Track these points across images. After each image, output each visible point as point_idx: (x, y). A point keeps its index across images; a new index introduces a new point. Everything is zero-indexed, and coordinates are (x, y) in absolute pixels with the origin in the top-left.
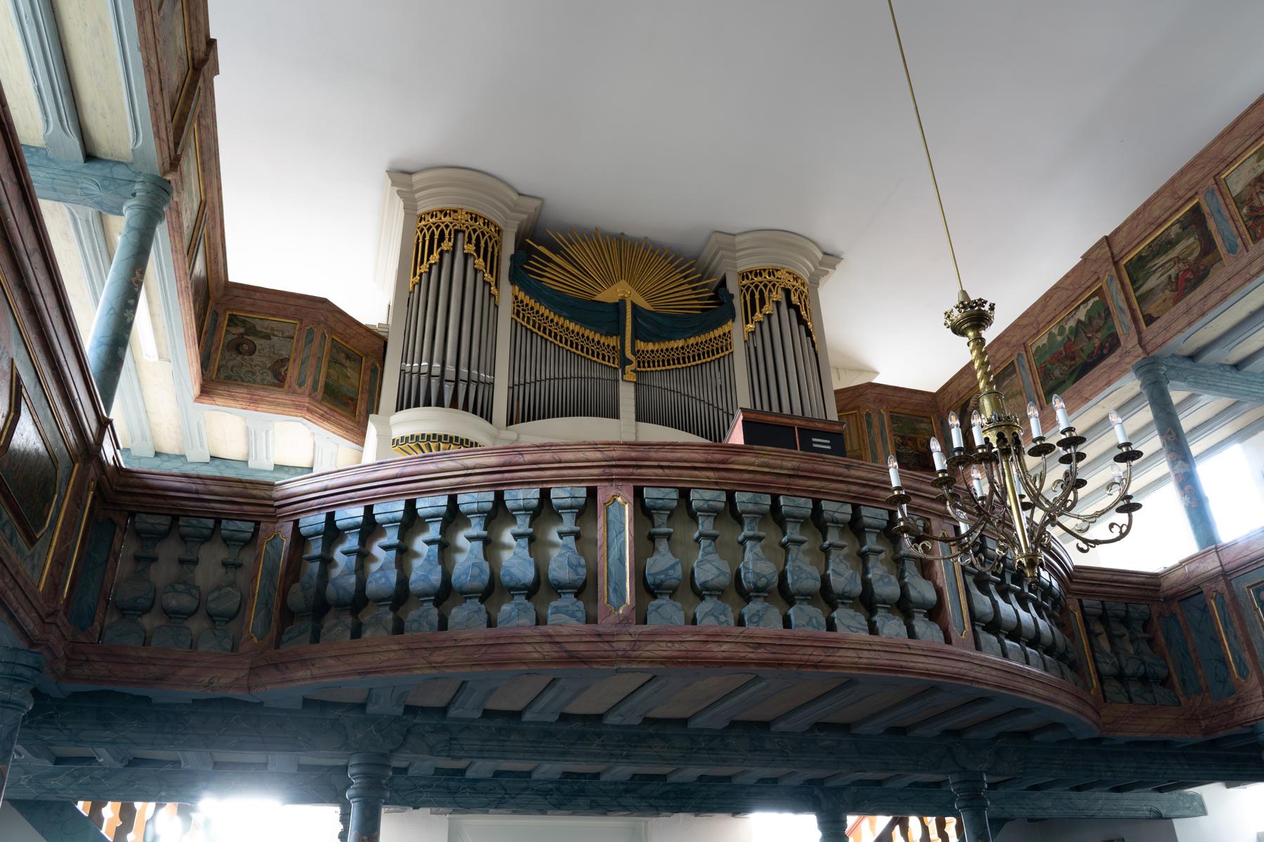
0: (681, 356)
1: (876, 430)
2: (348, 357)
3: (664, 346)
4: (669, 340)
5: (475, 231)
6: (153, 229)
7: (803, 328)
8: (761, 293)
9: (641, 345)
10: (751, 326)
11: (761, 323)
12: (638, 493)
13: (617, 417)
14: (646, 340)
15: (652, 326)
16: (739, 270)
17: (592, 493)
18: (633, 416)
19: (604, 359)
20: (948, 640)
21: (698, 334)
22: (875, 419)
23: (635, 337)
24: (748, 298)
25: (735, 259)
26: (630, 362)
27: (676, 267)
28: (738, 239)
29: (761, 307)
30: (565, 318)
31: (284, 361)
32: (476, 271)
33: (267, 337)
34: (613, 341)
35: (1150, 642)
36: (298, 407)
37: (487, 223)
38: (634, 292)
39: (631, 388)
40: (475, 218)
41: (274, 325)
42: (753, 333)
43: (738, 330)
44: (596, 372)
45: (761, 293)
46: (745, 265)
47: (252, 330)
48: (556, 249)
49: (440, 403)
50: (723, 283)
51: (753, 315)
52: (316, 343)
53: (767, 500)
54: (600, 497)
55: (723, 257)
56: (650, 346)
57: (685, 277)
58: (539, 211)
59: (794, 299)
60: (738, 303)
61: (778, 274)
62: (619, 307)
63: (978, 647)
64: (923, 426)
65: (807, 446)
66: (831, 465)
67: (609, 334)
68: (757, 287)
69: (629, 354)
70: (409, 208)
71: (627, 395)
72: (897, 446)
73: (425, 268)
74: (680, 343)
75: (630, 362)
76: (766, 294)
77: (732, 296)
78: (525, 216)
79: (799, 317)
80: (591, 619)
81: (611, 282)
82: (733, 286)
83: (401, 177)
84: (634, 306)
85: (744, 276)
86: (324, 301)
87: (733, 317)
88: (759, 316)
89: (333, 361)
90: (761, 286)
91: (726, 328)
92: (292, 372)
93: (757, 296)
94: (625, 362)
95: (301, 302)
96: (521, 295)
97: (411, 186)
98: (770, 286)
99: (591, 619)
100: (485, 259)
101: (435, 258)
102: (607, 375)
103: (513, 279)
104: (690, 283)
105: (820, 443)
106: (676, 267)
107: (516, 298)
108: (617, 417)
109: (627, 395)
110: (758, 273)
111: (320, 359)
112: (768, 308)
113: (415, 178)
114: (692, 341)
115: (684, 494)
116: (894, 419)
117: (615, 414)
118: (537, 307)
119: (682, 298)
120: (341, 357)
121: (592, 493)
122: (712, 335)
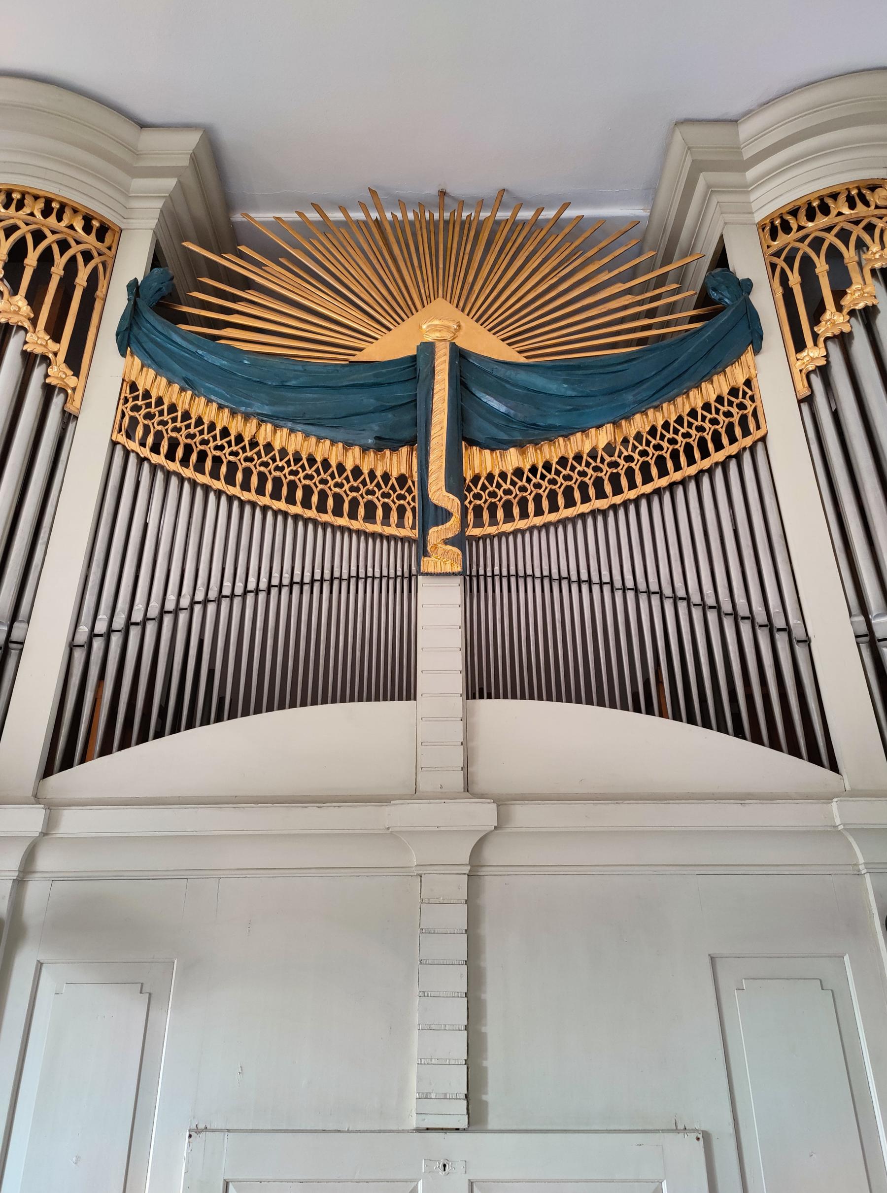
0: (606, 473)
3: (551, 452)
4: (567, 432)
5: (39, 236)
8: (834, 256)
9: (480, 461)
10: (813, 355)
11: (844, 340)
13: (409, 693)
14: (496, 445)
16: (759, 217)
18: (457, 683)
19: (370, 516)
23: (463, 434)
24: (794, 279)
25: (744, 189)
26: (443, 516)
28: (746, 130)
29: (839, 295)
30: (263, 419)
34: (397, 463)
38: (468, 323)
39: (454, 591)
42: (824, 371)
43: (773, 374)
44: (347, 556)
45: (834, 256)
48: (275, 254)
50: (721, 259)
51: (815, 320)
55: (711, 190)
56: (512, 459)
57: (651, 313)
60: (766, 302)
62: (414, 369)
67: (385, 443)
68: (817, 243)
69: (439, 493)
74: (602, 437)
75: (443, 516)
76: (849, 255)
77: (747, 286)
78: (170, 183)
81: (402, 309)
82: (748, 261)
84: (459, 356)
85: (775, 227)
87: (755, 338)
88: (834, 321)
90: (831, 238)
91: (737, 375)
93: (822, 267)
96: (147, 379)
98: (857, 231)
100: (34, 298)
102: (383, 560)
107: (133, 387)
108: (409, 693)
109: (440, 614)
110: (817, 207)
114: (639, 424)
117: (400, 684)
118: (183, 401)
119: (605, 319)
122: (696, 399)
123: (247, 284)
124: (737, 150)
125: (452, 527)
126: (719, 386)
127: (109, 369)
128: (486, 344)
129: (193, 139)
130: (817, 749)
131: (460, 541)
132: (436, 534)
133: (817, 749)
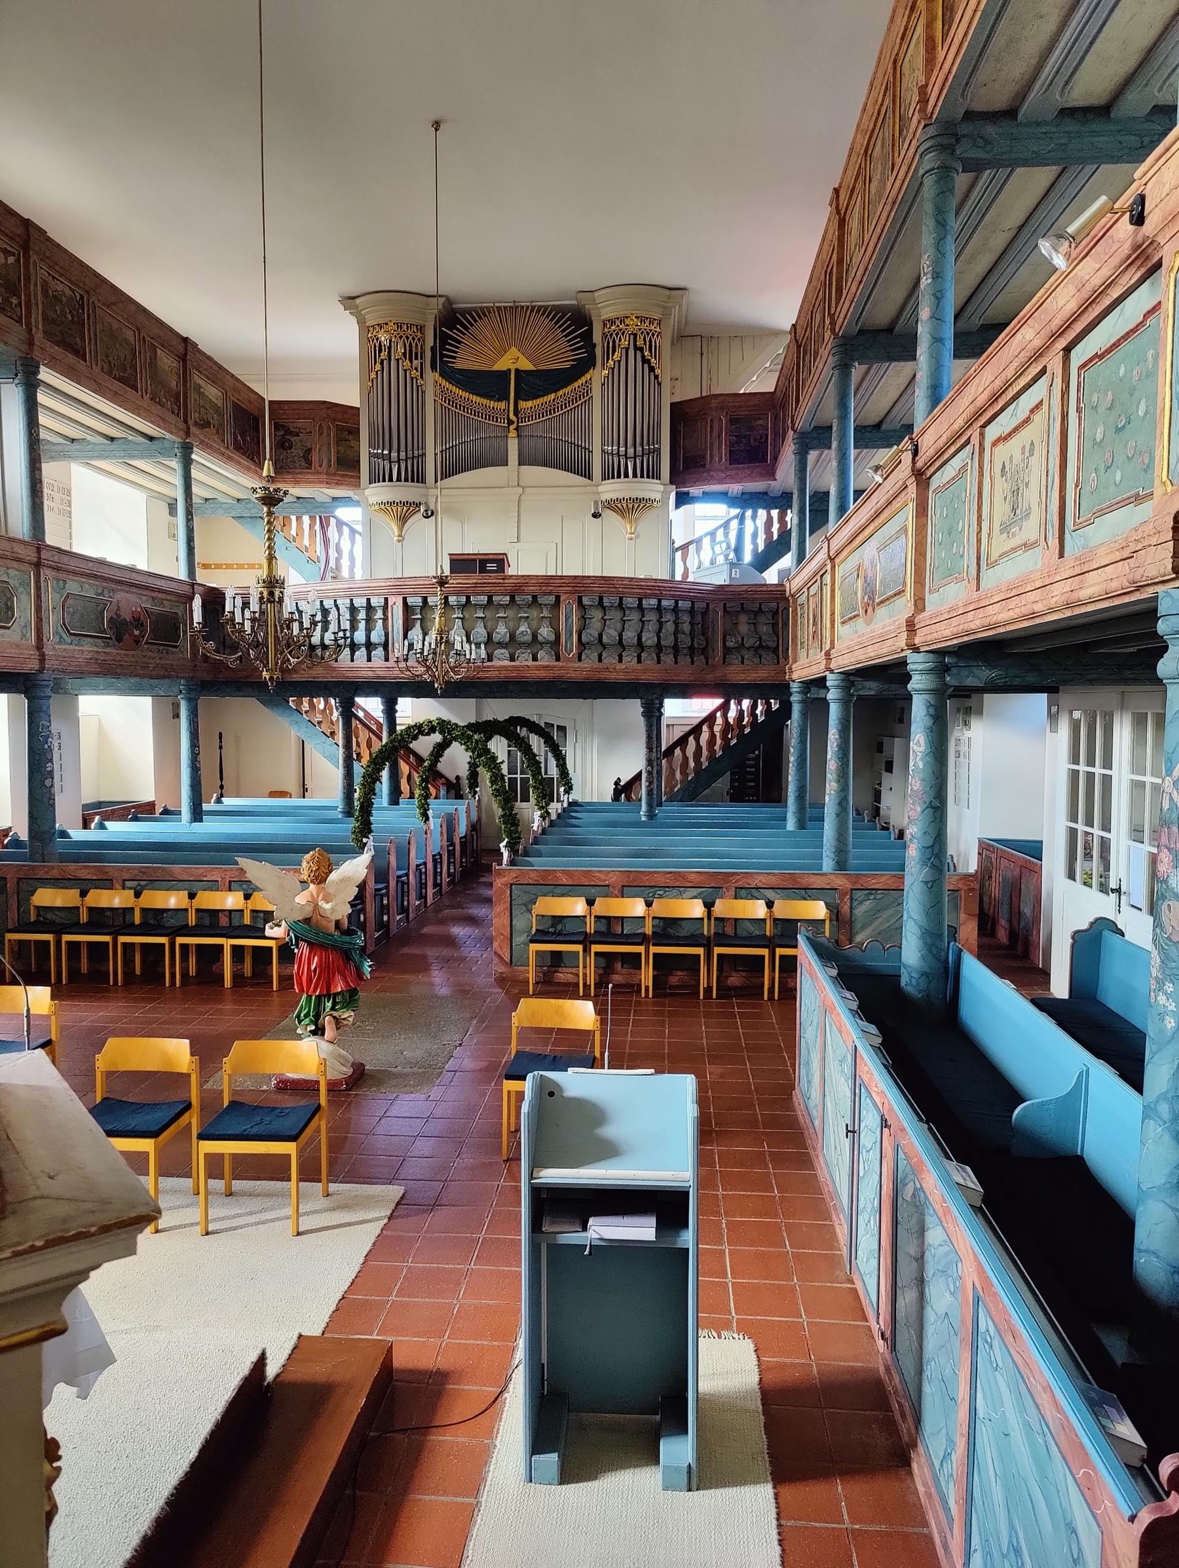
1: (715, 434)
2: (350, 433)
3: (539, 401)
6: (190, 471)
7: (646, 366)
9: (523, 405)
12: (405, 599)
15: (535, 384)
17: (386, 599)
18: (517, 463)
20: (558, 659)
21: (565, 386)
22: (716, 426)
27: (556, 323)
28: (596, 294)
31: (309, 451)
32: (405, 371)
33: (297, 435)
34: (502, 405)
35: (775, 625)
36: (321, 482)
37: (409, 326)
40: (399, 326)
41: (299, 425)
43: (597, 375)
46: (607, 314)
47: (289, 432)
49: (391, 480)
52: (325, 434)
53: (464, 599)
54: (390, 603)
56: (530, 404)
58: (449, 301)
59: (640, 343)
60: (598, 351)
61: (627, 321)
63: (580, 660)
64: (760, 422)
65: (483, 570)
66: (493, 579)
70: (361, 322)
71: (513, 446)
72: (732, 445)
73: (373, 376)
74: (553, 396)
79: (643, 356)
80: (387, 659)
83: (349, 301)
86: (325, 402)
87: (594, 365)
89: (339, 440)
91: (588, 376)
92: (315, 457)
94: (510, 422)
95: (311, 406)
97: (357, 307)
99: (387, 659)
101: (378, 367)
103: (433, 368)
104: (566, 336)
105: (491, 566)
106: (556, 323)
109: (513, 446)
110: (612, 322)
111: (329, 444)
112: (616, 356)
113: (358, 301)
114: (561, 392)
115: (425, 599)
116: (732, 421)
119: (559, 356)
120: (345, 435)
121: (386, 599)
122: (576, 384)
123: (460, 342)
124: (594, 300)
125: (514, 426)
126: (583, 380)
127: (432, 377)
128: (526, 365)
129: (442, 300)
130: (590, 478)
131: (517, 429)
132: (512, 427)
133: (590, 478)
